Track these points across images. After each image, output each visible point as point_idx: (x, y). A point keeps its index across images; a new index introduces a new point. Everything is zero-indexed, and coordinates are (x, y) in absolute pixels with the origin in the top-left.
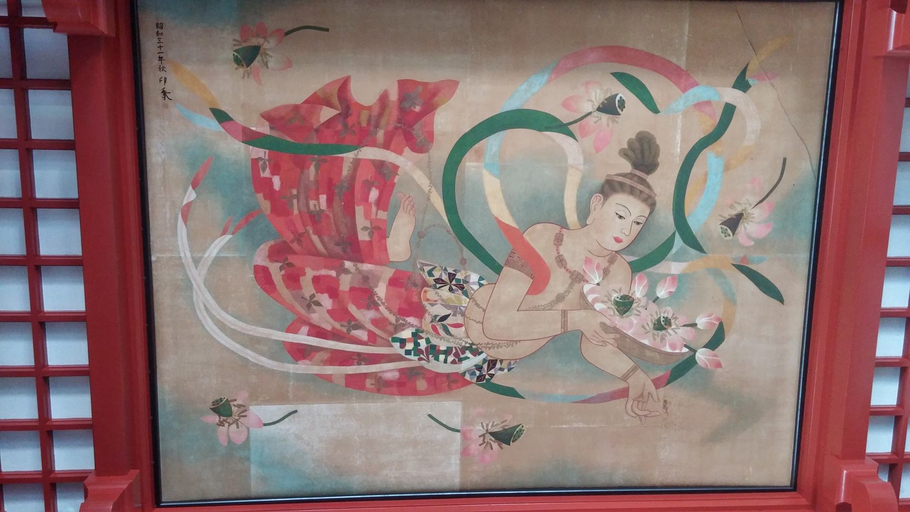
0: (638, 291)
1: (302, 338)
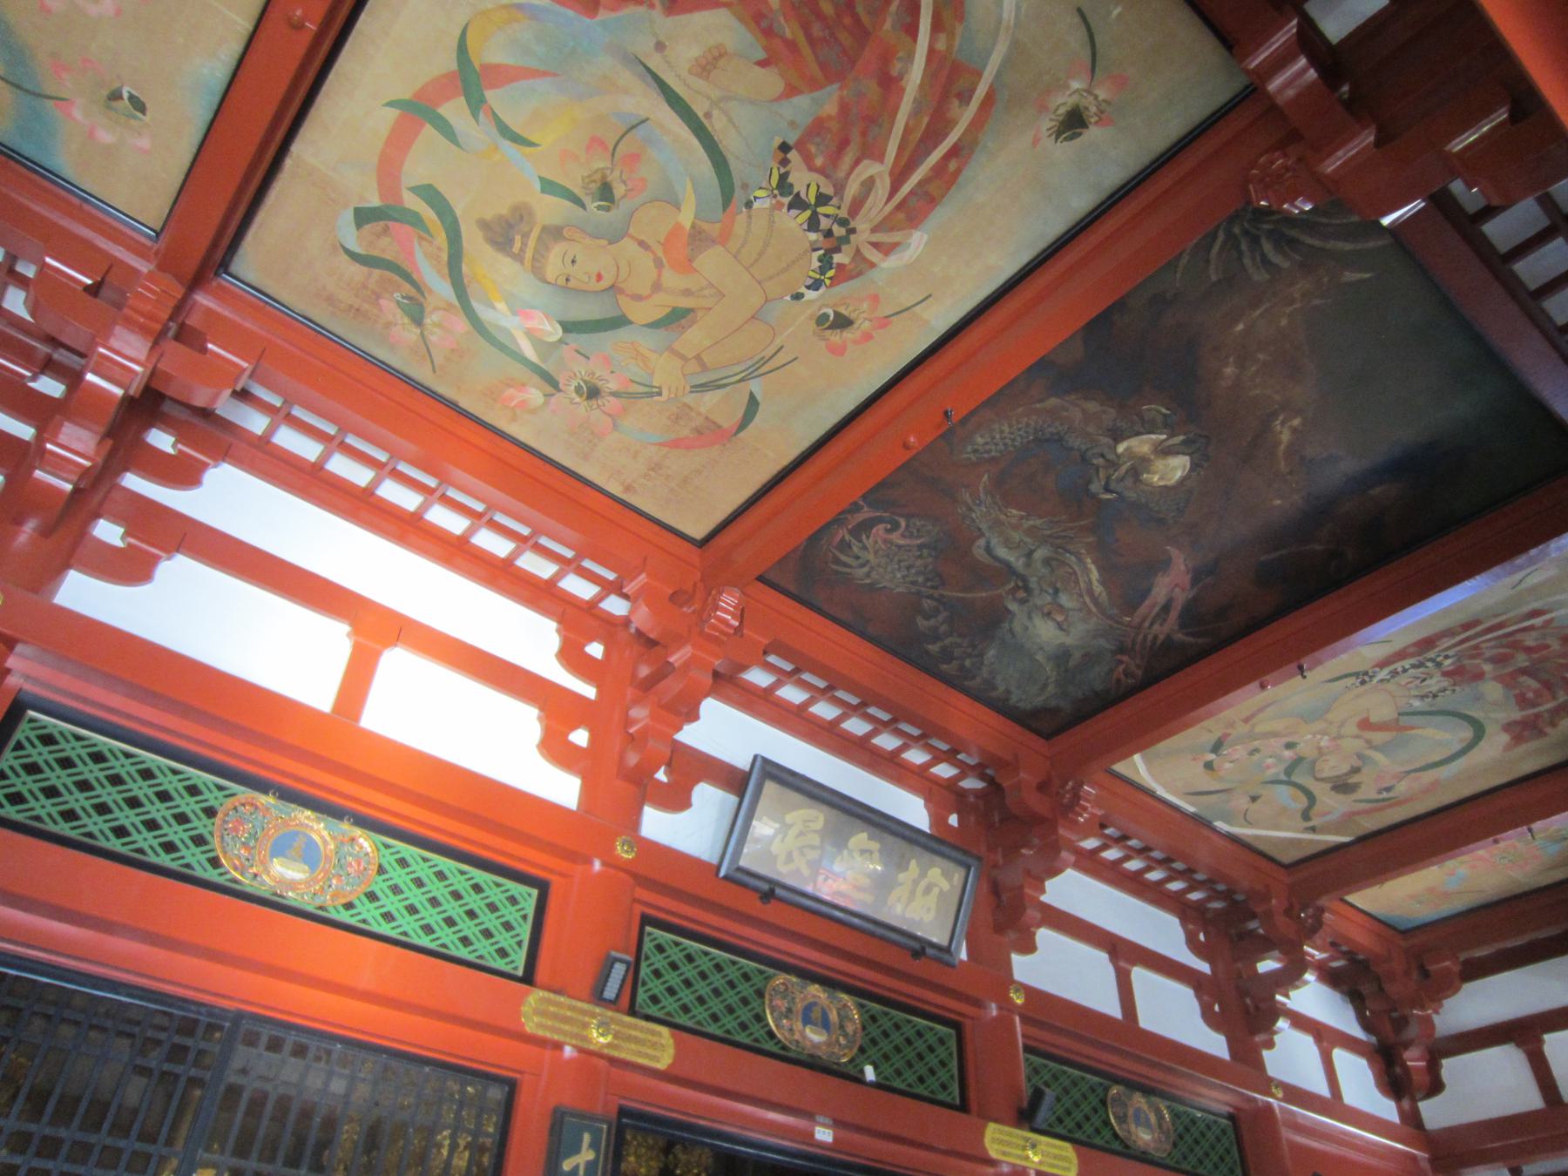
0: (1288, 754)
1: (1537, 621)
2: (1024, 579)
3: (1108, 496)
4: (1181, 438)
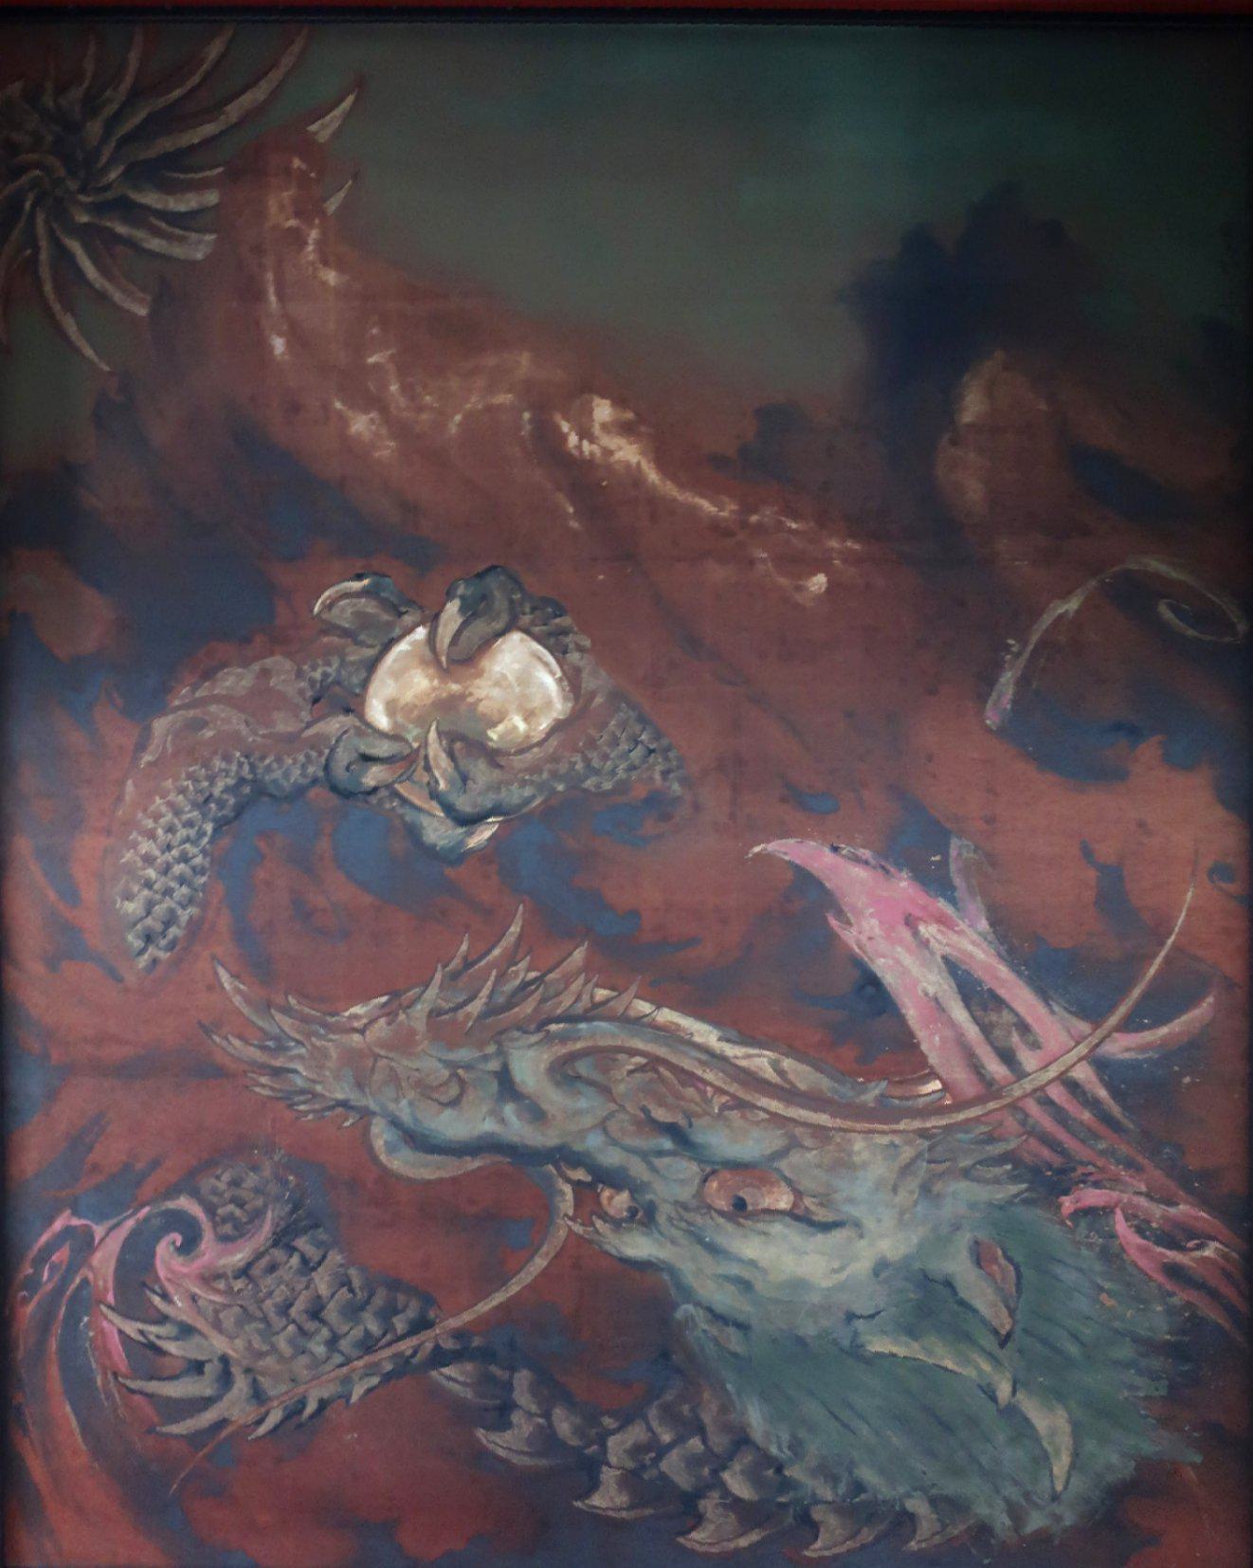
2: (565, 1156)
3: (483, 835)
4: (452, 608)
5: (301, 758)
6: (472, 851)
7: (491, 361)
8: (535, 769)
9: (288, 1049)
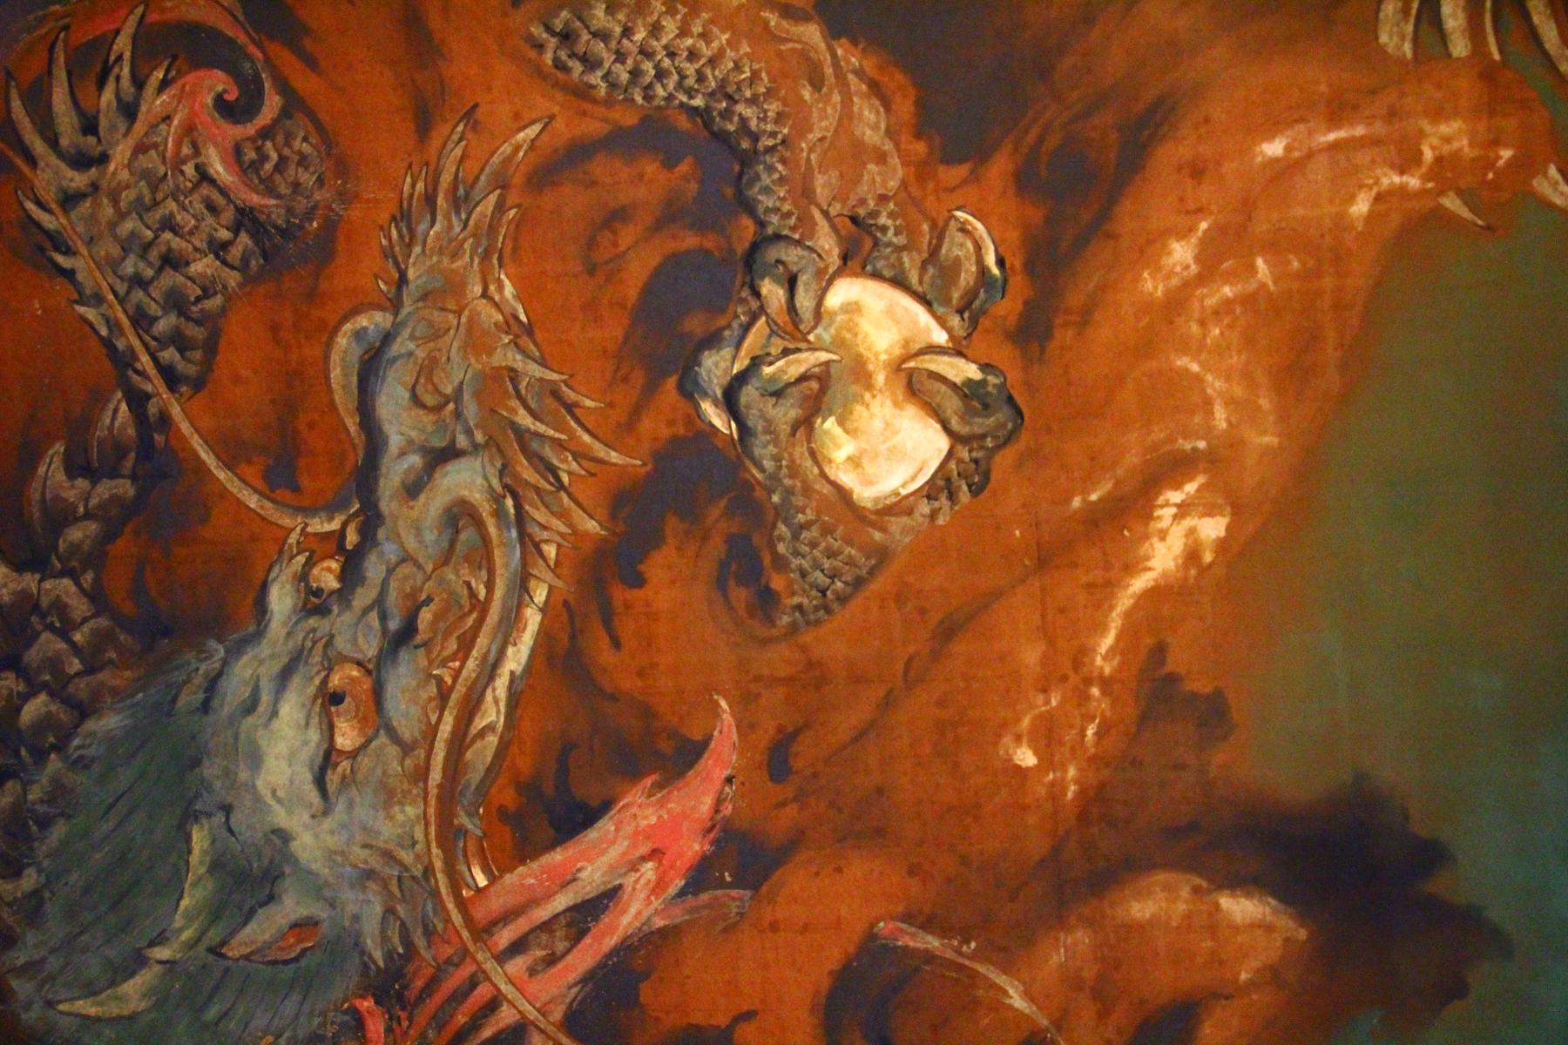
2: (371, 520)
3: (717, 418)
4: (972, 371)
5: (786, 207)
6: (697, 407)
7: (1264, 403)
8: (794, 471)
9: (458, 213)
